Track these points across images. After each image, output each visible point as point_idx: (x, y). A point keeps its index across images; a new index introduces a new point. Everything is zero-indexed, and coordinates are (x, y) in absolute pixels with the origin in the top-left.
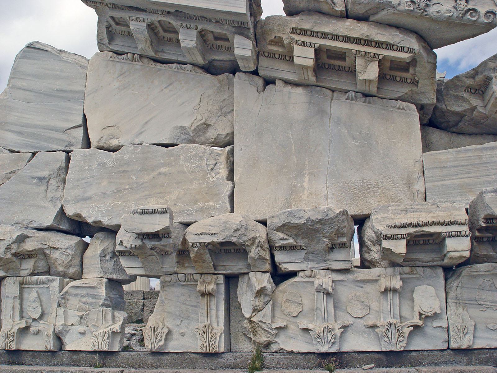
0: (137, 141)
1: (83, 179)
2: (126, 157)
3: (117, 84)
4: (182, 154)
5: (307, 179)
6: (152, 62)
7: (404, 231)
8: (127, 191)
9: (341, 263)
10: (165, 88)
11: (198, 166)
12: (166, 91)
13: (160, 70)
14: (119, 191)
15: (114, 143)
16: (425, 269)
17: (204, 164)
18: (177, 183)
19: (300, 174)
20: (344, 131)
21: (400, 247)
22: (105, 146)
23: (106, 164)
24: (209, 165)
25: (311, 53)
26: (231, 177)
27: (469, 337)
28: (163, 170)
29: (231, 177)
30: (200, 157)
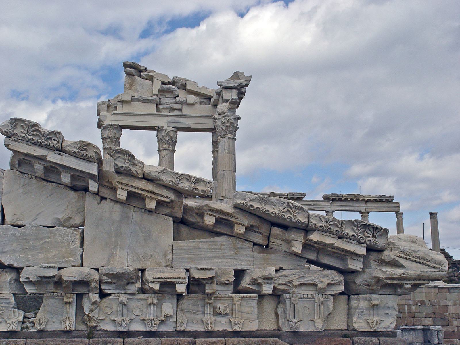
0: (33, 223)
1: (2, 241)
2: (27, 231)
3: (22, 190)
4: (57, 233)
5: (118, 250)
6: (42, 181)
7: (159, 280)
8: (27, 250)
9: (132, 291)
10: (50, 196)
11: (66, 239)
12: (49, 197)
13: (46, 186)
14: (23, 249)
15: (20, 223)
16: (169, 295)
17: (69, 238)
18: (54, 247)
19: (115, 247)
20: (138, 228)
21: (157, 287)
22: (14, 224)
23: (15, 234)
24: (71, 239)
25: (125, 194)
26: (82, 245)
27: (184, 326)
28: (47, 240)
29: (82, 245)
30: (67, 235)
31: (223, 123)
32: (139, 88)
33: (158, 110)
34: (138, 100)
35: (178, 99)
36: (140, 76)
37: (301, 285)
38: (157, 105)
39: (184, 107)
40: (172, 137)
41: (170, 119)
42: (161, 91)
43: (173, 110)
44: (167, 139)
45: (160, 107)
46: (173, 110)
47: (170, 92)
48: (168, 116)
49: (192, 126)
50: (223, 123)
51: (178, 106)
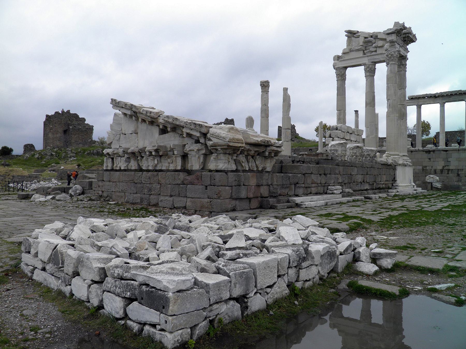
31: (387, 56)
32: (354, 44)
33: (364, 54)
34: (353, 51)
35: (374, 45)
36: (354, 37)
37: (190, 150)
38: (364, 51)
39: (378, 49)
40: (371, 68)
41: (369, 58)
42: (365, 42)
43: (372, 52)
44: (368, 69)
45: (365, 52)
46: (372, 52)
47: (370, 42)
48: (368, 56)
49: (382, 59)
50: (387, 56)
51: (374, 49)
